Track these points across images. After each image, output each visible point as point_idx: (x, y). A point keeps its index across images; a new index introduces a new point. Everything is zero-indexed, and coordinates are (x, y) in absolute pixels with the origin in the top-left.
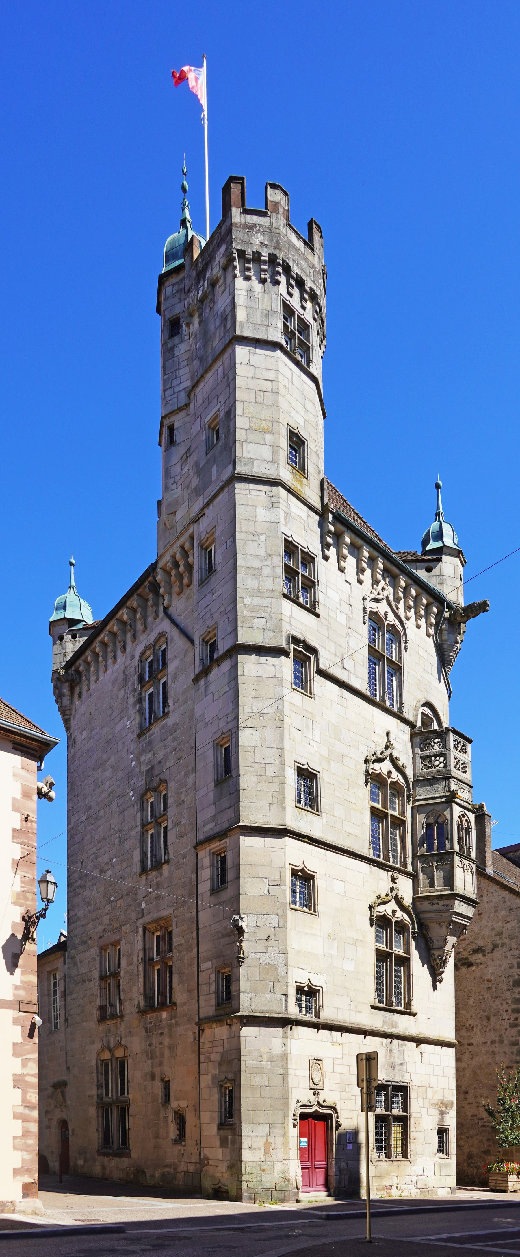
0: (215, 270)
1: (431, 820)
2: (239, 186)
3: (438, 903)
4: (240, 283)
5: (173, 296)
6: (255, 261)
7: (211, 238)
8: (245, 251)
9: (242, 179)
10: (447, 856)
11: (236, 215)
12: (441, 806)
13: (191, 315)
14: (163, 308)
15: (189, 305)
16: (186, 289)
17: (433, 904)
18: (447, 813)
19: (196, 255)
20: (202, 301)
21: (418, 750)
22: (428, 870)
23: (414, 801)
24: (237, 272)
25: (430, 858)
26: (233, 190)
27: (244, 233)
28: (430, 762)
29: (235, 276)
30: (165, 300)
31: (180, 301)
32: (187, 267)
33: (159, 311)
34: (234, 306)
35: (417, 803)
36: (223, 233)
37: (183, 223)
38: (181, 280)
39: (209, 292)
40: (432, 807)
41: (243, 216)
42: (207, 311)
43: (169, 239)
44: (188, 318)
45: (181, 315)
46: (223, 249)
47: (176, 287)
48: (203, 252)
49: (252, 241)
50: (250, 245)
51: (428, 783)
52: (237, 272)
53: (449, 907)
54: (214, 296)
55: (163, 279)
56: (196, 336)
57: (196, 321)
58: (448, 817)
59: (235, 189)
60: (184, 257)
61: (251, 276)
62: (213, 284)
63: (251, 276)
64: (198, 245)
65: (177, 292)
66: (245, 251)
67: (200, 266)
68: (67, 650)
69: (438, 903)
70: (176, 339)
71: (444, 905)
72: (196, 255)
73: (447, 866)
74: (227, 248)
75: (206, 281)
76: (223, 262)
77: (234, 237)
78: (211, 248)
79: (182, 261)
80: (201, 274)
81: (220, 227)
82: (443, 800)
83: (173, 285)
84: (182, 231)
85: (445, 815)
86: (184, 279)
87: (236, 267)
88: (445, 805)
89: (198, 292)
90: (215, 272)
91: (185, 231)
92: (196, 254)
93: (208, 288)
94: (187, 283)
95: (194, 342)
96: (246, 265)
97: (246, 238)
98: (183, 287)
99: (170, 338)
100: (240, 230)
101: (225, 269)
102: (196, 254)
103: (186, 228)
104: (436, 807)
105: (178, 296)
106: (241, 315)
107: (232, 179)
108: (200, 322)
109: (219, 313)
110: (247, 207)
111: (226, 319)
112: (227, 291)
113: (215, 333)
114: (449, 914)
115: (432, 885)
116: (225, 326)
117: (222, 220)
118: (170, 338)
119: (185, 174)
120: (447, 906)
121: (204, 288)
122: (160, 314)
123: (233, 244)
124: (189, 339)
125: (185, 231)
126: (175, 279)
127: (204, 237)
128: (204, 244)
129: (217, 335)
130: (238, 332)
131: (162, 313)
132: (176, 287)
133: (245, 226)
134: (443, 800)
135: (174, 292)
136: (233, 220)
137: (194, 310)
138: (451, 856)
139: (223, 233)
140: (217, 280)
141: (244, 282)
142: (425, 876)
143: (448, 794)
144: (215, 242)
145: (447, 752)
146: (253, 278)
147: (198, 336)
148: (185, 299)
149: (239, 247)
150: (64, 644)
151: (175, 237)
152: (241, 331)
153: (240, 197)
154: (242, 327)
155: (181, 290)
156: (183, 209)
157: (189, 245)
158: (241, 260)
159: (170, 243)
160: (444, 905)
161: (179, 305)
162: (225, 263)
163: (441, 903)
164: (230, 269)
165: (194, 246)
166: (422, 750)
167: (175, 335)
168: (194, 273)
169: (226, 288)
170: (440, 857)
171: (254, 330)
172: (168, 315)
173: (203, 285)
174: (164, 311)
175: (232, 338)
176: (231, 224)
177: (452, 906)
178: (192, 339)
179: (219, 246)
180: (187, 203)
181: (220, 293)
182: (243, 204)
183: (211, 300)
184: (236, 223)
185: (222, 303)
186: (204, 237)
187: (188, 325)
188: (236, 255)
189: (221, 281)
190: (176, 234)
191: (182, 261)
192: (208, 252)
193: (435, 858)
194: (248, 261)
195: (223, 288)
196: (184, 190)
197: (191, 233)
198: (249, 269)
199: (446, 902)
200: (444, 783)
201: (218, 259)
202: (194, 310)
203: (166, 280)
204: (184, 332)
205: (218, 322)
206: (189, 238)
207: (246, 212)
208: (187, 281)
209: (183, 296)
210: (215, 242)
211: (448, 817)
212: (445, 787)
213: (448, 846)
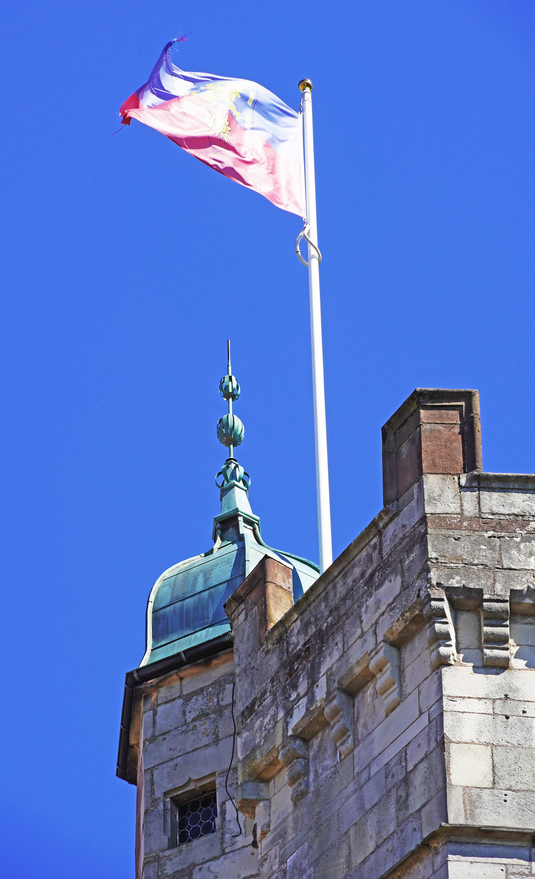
0: (360, 647)
2: (455, 416)
4: (461, 681)
5: (186, 727)
6: (525, 615)
7: (336, 563)
8: (480, 592)
9: (468, 396)
11: (442, 494)
13: (261, 778)
14: (142, 764)
15: (252, 750)
16: (240, 707)
19: (277, 614)
20: (304, 736)
24: (449, 650)
26: (425, 428)
27: (477, 543)
29: (444, 662)
30: (152, 739)
31: (216, 741)
32: (241, 646)
33: (127, 770)
34: (440, 745)
36: (389, 543)
37: (227, 526)
38: (219, 684)
39: (336, 712)
41: (469, 497)
42: (328, 762)
43: (167, 574)
44: (250, 786)
45: (219, 781)
46: (392, 587)
47: (197, 705)
48: (303, 602)
49: (506, 563)
50: (500, 575)
52: (449, 650)
54: (354, 722)
55: (138, 686)
56: (282, 835)
57: (281, 794)
59: (437, 428)
60: (231, 620)
61: (507, 660)
62: (351, 691)
63: (507, 660)
64: (289, 584)
65: (203, 715)
66: (480, 592)
67: (297, 641)
70: (200, 847)
72: (277, 614)
74: (405, 587)
75: (323, 682)
76: (392, 625)
77: (432, 554)
78: (341, 590)
79: (226, 628)
80: (298, 664)
81: (375, 528)
83: (187, 698)
84: (224, 550)
86: (230, 678)
87: (447, 636)
89: (289, 713)
90: (356, 654)
91: (235, 547)
92: (279, 608)
93: (329, 699)
94: (243, 692)
95: (275, 851)
96: (487, 629)
97: (484, 554)
98: (228, 700)
99: (172, 845)
100: (457, 533)
101: (398, 644)
102: (279, 608)
103: (241, 539)
105: (205, 726)
106: (466, 769)
107: (420, 399)
108: (298, 798)
109: (375, 769)
110: (483, 469)
111: (406, 781)
112: (410, 705)
113: (359, 826)
116: (403, 803)
117: (386, 512)
118: (172, 845)
119: (229, 395)
121: (312, 700)
122: (133, 781)
123: (434, 575)
124: (255, 844)
125: (235, 547)
126: (193, 679)
127: (312, 559)
128: (308, 578)
129: (371, 830)
130: (456, 816)
131: (141, 777)
132: (197, 705)
133: (481, 521)
135: (189, 717)
136: (428, 509)
137: (273, 763)
139: (389, 543)
140: (369, 677)
141: (481, 677)
144: (357, 571)
146: (518, 663)
147: (291, 835)
148: (236, 734)
149: (455, 582)
151: (195, 567)
152: (471, 813)
153: (458, 445)
154: (472, 802)
155: (219, 710)
156: (226, 490)
157: (251, 587)
158: (465, 617)
159: (173, 582)
161: (211, 750)
162: (399, 627)
164: (420, 642)
165: (270, 588)
167: (196, 834)
168: (274, 662)
169: (402, 696)
171: (522, 808)
172: (164, 783)
173: (310, 693)
174: (150, 771)
175: (433, 836)
176: (423, 520)
178: (263, 844)
179: (371, 583)
180: (240, 472)
181: (383, 713)
182: (470, 463)
183: (344, 732)
184: (442, 520)
185: (386, 735)
186: (312, 559)
187: (248, 806)
188: (445, 605)
189: (381, 681)
190: (198, 559)
191: (226, 628)
192: (325, 610)
194: (495, 618)
195: (395, 696)
196: (229, 437)
197: (254, 555)
198: (501, 641)
201: (368, 619)
202: (273, 763)
203: (157, 687)
204: (233, 827)
205: (371, 794)
206: (250, 567)
207: (480, 484)
208: (242, 686)
209: (225, 728)
210: (357, 571)
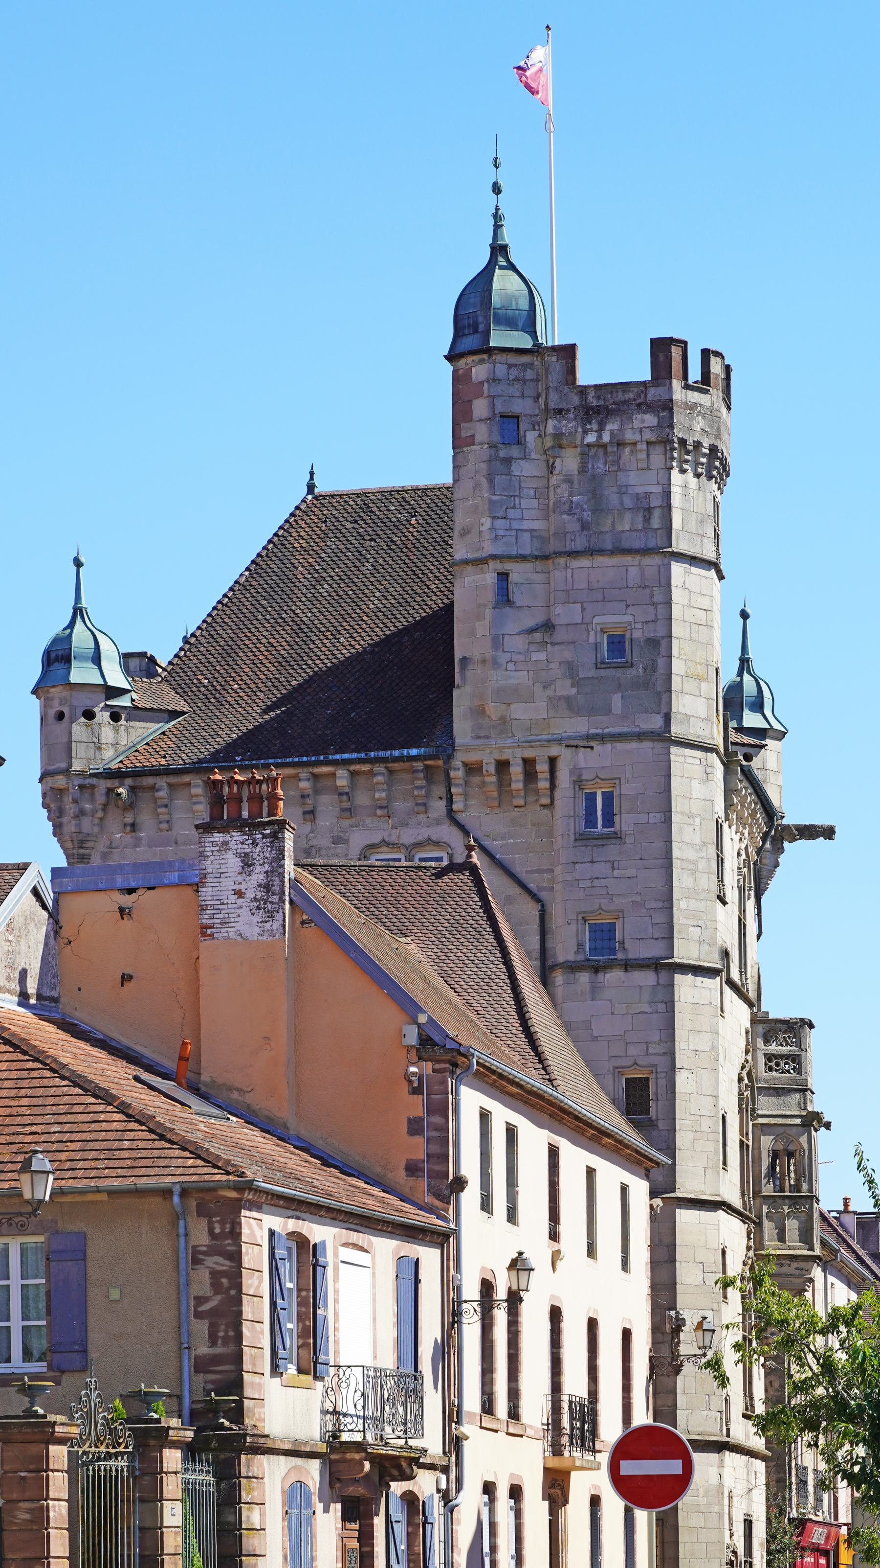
1: (780, 1146)
3: (789, 1265)
10: (803, 1201)
12: (794, 1129)
17: (782, 1265)
18: (803, 1140)
21: (760, 1042)
22: (776, 1217)
23: (756, 1119)
25: (780, 1201)
28: (777, 1064)
35: (761, 1121)
40: (782, 1129)
51: (775, 1093)
53: (804, 1272)
58: (806, 1146)
68: (103, 740)
69: (789, 1265)
71: (797, 1269)
73: (803, 1215)
82: (798, 1121)
85: (800, 1144)
88: (800, 1128)
104: (787, 1129)
114: (801, 1280)
115: (782, 1238)
120: (802, 1269)
134: (798, 1121)
138: (809, 1201)
142: (772, 1225)
143: (804, 1113)
145: (803, 1053)
150: (95, 727)
160: (797, 1269)
163: (795, 1265)
166: (767, 1042)
170: (793, 1202)
177: (809, 1271)
193: (787, 1201)
199: (802, 1265)
200: (797, 1096)
211: (806, 1146)
212: (799, 1103)
213: (805, 1187)
